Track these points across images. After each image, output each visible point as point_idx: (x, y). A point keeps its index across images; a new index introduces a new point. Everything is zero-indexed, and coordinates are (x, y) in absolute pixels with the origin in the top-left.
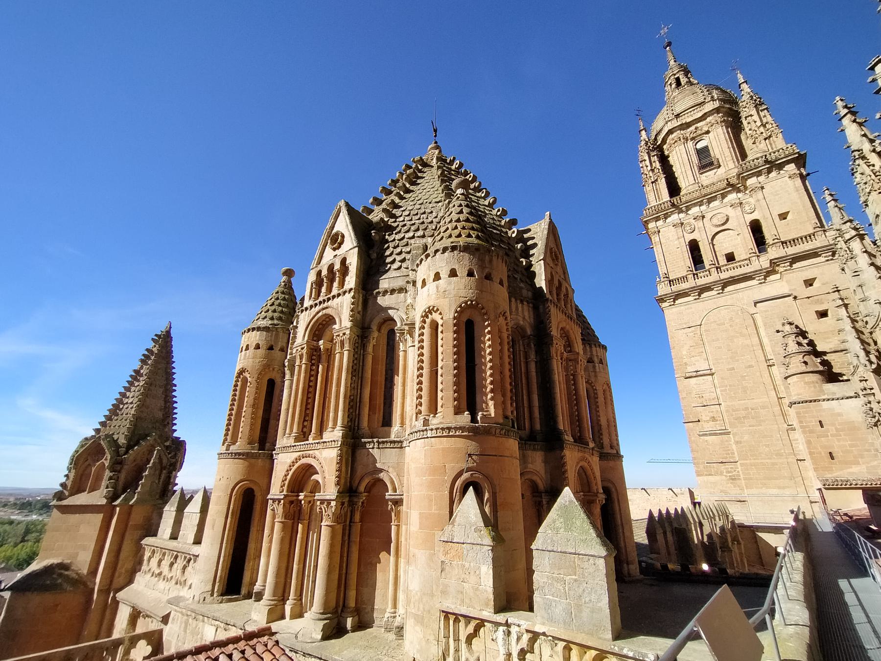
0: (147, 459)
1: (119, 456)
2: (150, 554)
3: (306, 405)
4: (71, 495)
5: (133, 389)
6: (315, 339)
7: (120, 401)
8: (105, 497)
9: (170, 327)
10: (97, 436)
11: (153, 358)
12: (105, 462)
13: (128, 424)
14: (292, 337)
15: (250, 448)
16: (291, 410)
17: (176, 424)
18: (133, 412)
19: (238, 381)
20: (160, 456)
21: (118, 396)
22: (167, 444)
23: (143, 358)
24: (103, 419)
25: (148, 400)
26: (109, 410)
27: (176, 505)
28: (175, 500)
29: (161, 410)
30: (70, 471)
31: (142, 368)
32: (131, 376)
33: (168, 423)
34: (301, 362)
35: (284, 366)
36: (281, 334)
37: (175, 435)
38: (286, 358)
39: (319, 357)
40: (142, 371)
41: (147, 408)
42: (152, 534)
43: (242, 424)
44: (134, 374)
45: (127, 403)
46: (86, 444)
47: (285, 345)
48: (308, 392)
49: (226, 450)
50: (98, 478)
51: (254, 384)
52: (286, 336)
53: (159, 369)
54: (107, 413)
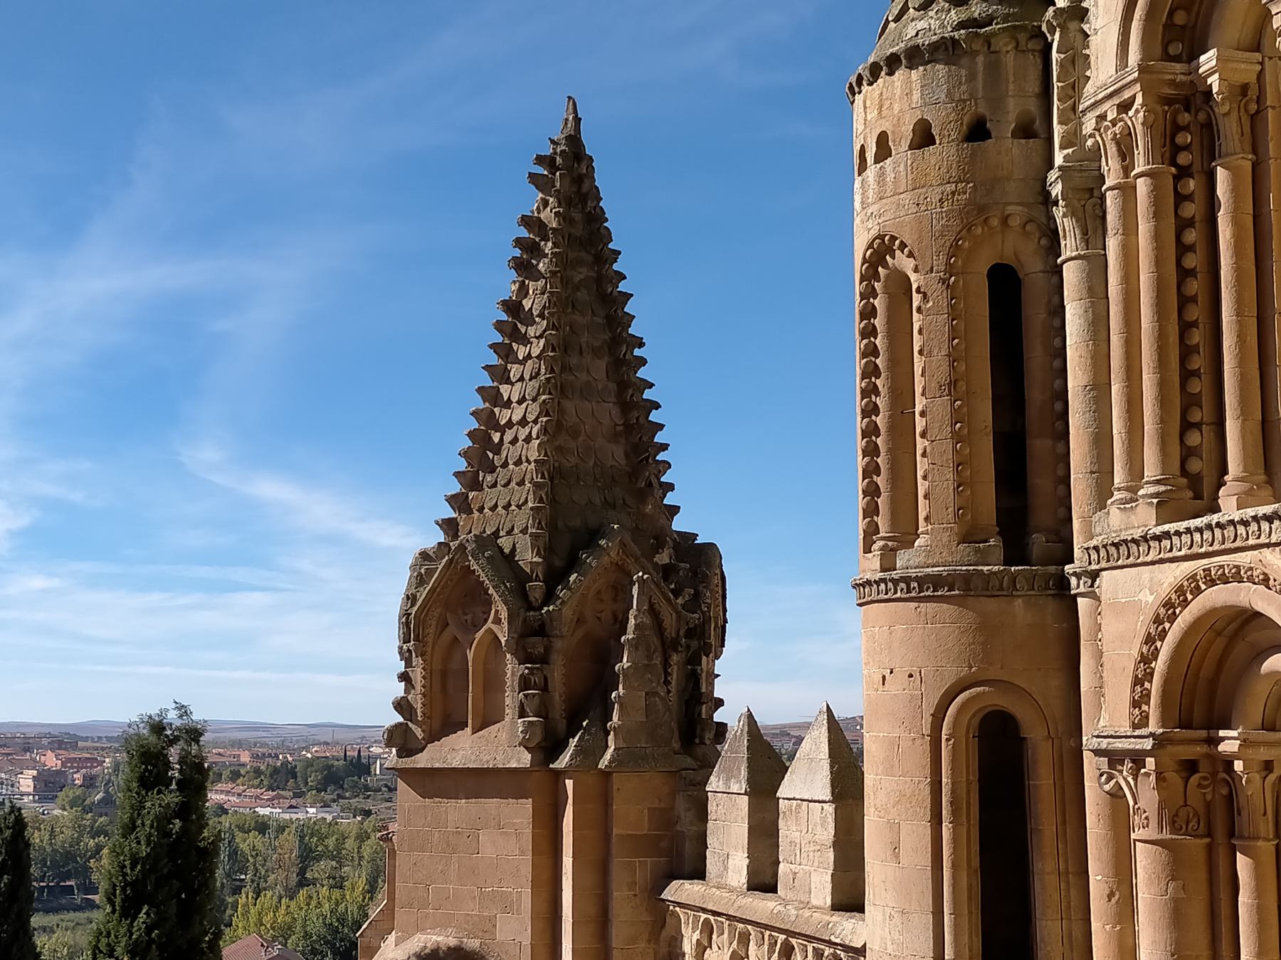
0: (615, 617)
1: (530, 607)
2: (696, 936)
3: (1183, 360)
4: (433, 737)
5: (515, 371)
6: (1176, 48)
7: (487, 420)
8: (524, 744)
9: (577, 120)
10: (454, 545)
11: (548, 247)
12: (494, 627)
13: (531, 497)
14: (1062, 65)
15: (973, 558)
16: (1116, 389)
17: (671, 487)
18: (534, 455)
19: (874, 294)
20: (651, 606)
21: (480, 404)
22: (664, 558)
23: (517, 252)
24: (456, 487)
25: (569, 405)
26: (465, 454)
27: (744, 772)
28: (734, 753)
29: (614, 437)
30: (408, 663)
31: (523, 291)
32: (499, 326)
33: (650, 485)
34: (1127, 170)
35: (1048, 201)
36: (1010, 60)
37: (679, 524)
38: (1050, 165)
39: (1209, 132)
40: (527, 304)
41: (575, 434)
42: (687, 868)
43: (922, 466)
44: (504, 317)
45: (510, 424)
46: (430, 572)
47: (1033, 106)
48: (1184, 301)
49: (883, 570)
50: (492, 684)
51: (939, 296)
52: (1035, 62)
53: (577, 288)
54: (462, 465)
